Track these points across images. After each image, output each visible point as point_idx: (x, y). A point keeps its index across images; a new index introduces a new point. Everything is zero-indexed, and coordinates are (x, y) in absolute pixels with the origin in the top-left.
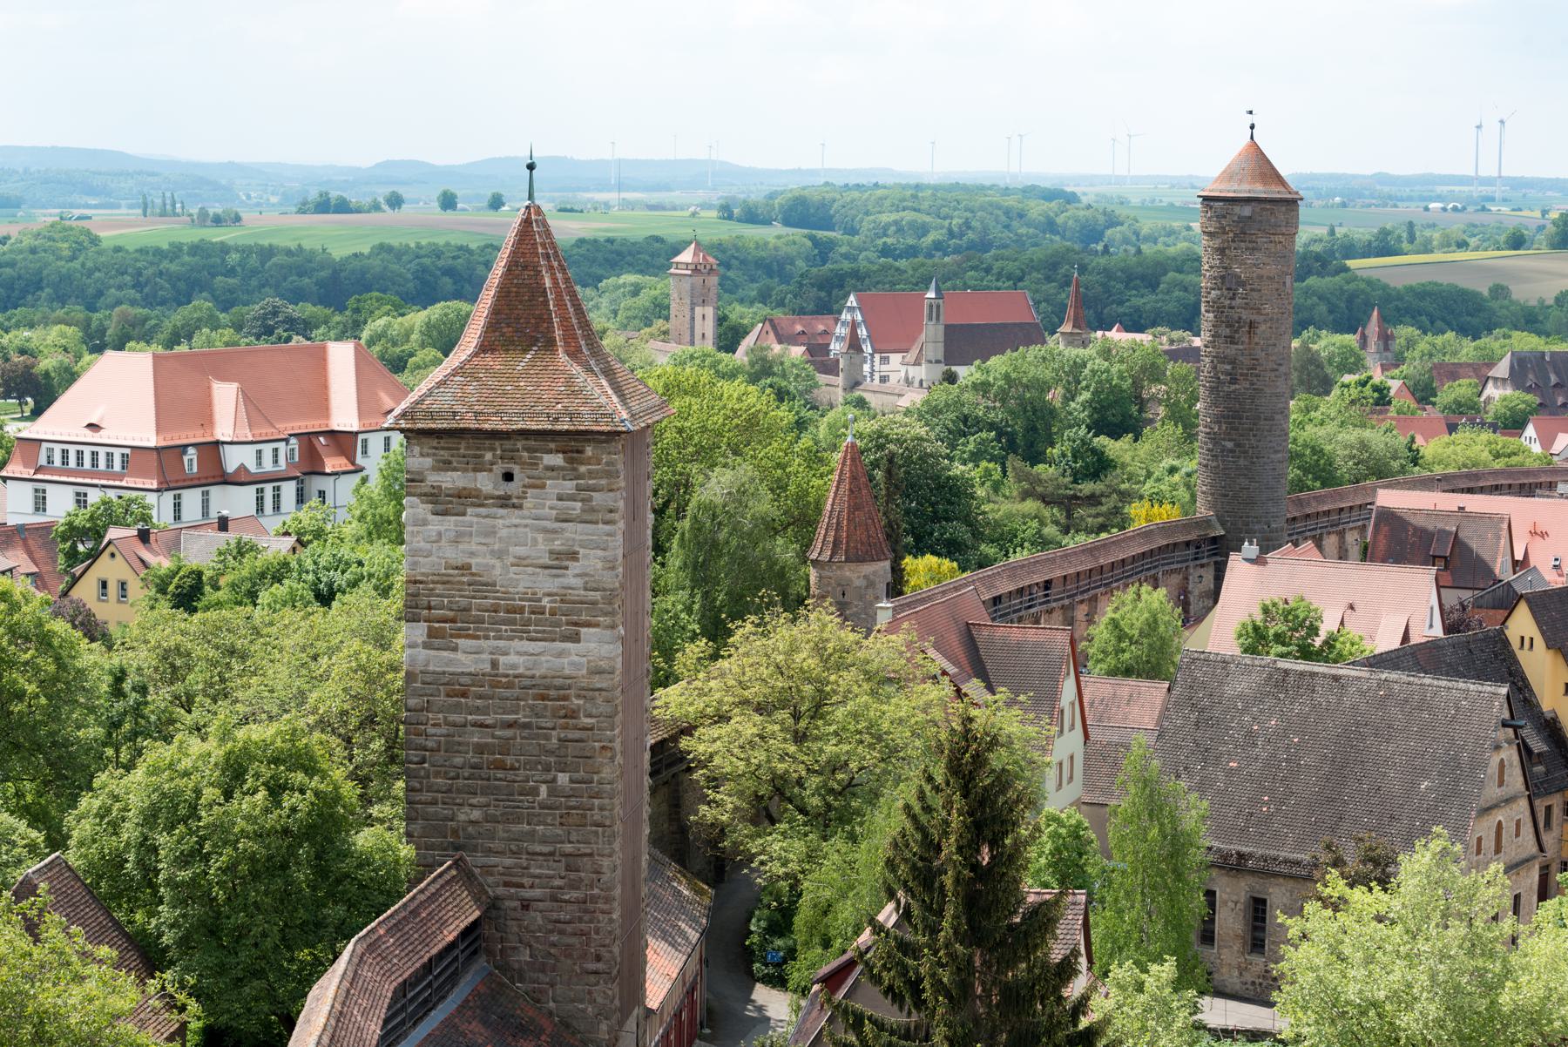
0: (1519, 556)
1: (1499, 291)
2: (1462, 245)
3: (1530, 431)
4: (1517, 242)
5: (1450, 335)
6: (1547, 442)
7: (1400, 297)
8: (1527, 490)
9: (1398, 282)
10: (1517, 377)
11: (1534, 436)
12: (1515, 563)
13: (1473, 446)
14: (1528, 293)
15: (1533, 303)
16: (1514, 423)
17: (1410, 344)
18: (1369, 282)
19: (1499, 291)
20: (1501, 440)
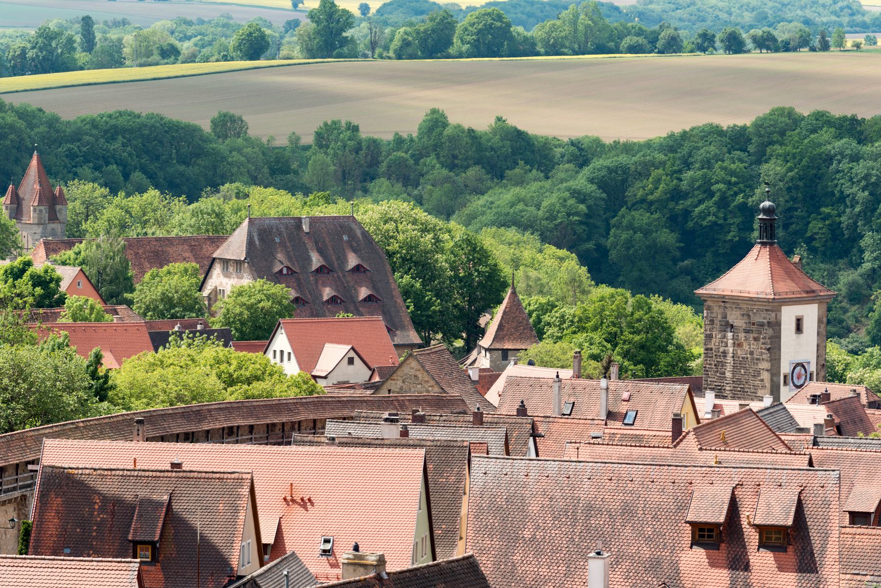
0: (268, 538)
1: (228, 125)
2: (170, 53)
3: (281, 341)
4: (256, 46)
5: (152, 194)
6: (307, 356)
7: (76, 136)
8: (278, 434)
9: (72, 112)
10: (258, 258)
11: (287, 348)
12: (263, 549)
13: (195, 367)
14: (271, 128)
15: (282, 141)
16: (255, 330)
17: (91, 210)
18: (23, 114)
19: (228, 125)
20: (235, 355)
